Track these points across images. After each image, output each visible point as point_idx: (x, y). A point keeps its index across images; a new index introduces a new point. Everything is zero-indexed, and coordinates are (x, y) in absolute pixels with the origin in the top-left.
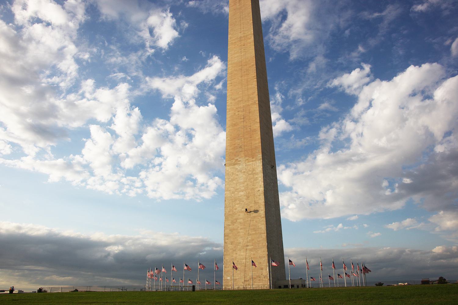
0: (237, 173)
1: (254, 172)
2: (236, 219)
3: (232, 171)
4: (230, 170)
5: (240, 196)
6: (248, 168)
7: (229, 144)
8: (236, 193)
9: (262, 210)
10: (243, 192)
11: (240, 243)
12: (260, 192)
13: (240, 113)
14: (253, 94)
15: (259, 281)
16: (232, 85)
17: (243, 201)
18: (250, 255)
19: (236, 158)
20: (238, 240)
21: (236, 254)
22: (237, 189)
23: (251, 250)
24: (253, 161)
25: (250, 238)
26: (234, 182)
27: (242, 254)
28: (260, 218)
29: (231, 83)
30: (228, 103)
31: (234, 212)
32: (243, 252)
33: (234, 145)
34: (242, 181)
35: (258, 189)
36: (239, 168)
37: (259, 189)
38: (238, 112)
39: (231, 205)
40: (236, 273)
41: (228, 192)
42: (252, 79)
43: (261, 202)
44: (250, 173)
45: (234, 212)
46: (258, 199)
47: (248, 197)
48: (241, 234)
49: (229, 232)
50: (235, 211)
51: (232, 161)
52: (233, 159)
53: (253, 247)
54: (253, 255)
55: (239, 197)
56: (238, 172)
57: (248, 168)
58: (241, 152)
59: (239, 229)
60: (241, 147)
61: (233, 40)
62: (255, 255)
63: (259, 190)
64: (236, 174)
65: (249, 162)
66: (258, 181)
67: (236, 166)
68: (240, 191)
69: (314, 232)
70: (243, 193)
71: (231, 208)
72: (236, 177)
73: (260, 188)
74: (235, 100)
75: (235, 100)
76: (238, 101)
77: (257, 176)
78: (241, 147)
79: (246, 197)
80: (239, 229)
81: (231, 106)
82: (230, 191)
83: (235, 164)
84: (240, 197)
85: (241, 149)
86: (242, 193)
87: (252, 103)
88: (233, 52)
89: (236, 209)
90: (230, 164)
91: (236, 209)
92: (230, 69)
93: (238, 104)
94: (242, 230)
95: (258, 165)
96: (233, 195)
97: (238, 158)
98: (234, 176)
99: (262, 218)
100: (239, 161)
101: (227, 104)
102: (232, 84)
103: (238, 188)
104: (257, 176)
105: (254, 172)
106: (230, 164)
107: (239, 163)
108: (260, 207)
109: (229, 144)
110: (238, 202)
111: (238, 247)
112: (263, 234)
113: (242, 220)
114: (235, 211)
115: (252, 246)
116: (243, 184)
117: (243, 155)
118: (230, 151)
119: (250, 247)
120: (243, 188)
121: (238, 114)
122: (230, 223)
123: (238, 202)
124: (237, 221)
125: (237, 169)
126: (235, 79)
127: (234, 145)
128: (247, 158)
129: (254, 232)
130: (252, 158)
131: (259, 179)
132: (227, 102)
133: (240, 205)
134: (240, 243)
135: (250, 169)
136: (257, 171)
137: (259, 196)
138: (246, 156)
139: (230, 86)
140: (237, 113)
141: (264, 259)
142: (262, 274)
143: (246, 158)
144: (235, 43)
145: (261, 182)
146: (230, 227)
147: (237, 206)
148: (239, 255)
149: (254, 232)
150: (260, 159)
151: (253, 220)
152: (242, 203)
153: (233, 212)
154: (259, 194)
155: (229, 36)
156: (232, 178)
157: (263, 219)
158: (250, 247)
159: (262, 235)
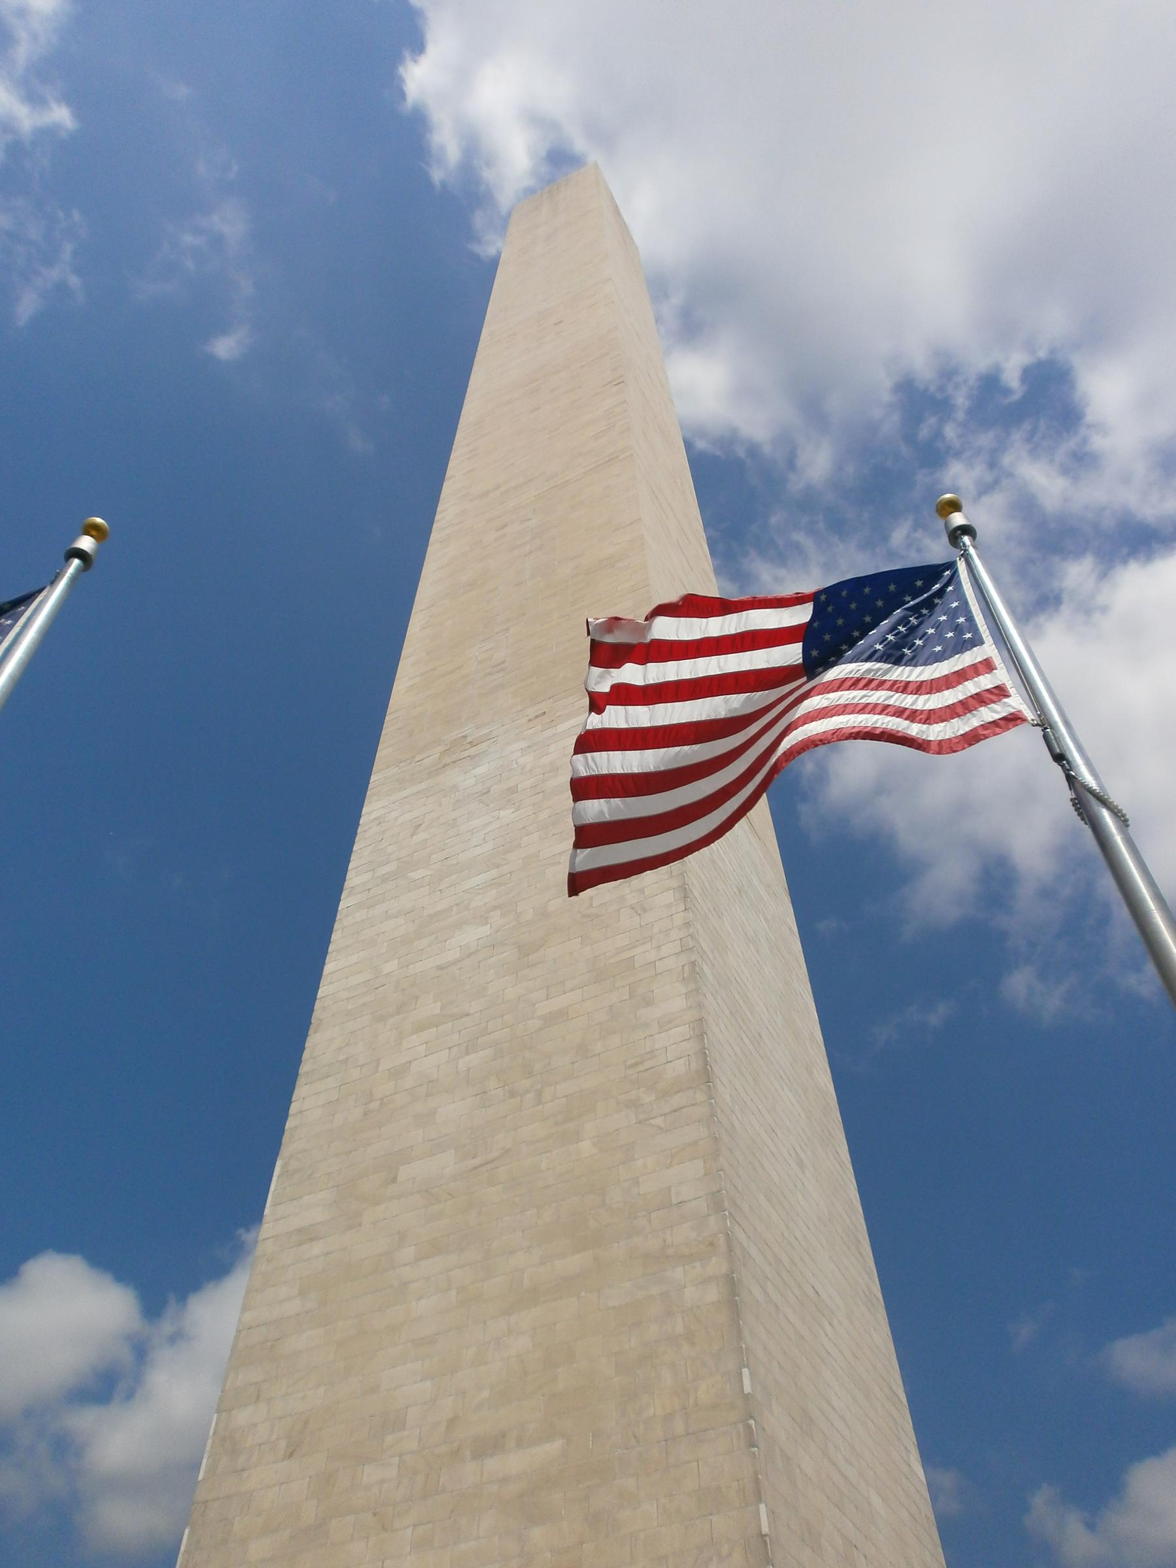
10: (485, 920)
26: (416, 875)
28: (648, 1098)
43: (652, 956)
51: (418, 758)
55: (440, 968)
70: (484, 931)
84: (455, 963)
91: (398, 1073)
96: (391, 966)
107: (472, 751)
108: (648, 1002)
116: (498, 866)
124: (394, 1180)
157: (678, 1100)
158: (515, 1462)
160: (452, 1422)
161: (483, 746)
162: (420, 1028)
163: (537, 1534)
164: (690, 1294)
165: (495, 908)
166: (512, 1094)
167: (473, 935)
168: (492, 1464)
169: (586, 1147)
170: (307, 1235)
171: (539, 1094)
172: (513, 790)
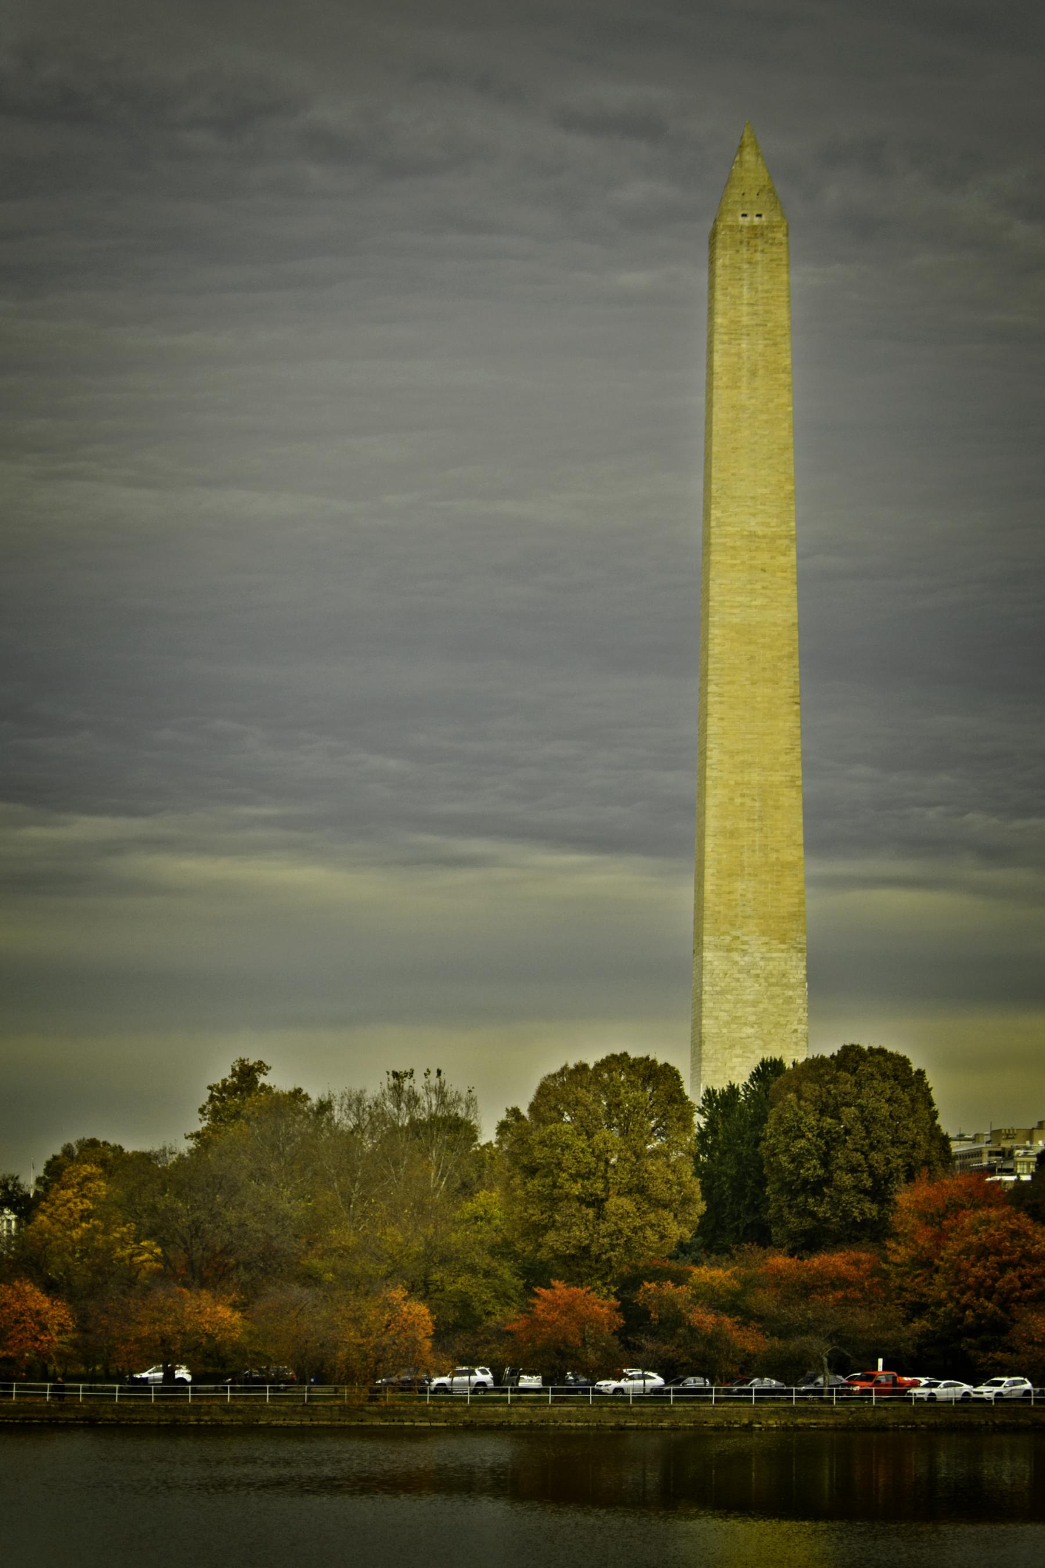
1: (785, 981)
3: (723, 967)
4: (716, 963)
5: (743, 1035)
13: (748, 801)
14: (786, 753)
24: (782, 951)
26: (729, 997)
29: (720, 695)
36: (743, 963)
37: (796, 1027)
38: (743, 796)
39: (719, 1056)
41: (712, 1022)
44: (773, 980)
52: (727, 933)
56: (739, 972)
57: (769, 968)
58: (749, 917)
61: (726, 536)
63: (796, 1031)
65: (769, 951)
66: (793, 1006)
67: (736, 956)
68: (745, 1024)
69: (988, 1179)
70: (753, 1030)
72: (734, 984)
74: (732, 754)
75: (732, 754)
76: (742, 762)
77: (790, 993)
81: (721, 771)
82: (717, 1018)
83: (729, 950)
86: (749, 1031)
87: (783, 778)
88: (724, 581)
89: (733, 1068)
90: (716, 946)
91: (733, 1068)
92: (717, 641)
95: (794, 963)
96: (725, 1031)
98: (727, 980)
100: (744, 943)
101: (709, 762)
102: (724, 699)
104: (790, 993)
105: (785, 981)
106: (716, 946)
117: (754, 929)
118: (717, 909)
121: (742, 804)
123: (738, 1051)
126: (732, 683)
127: (729, 893)
130: (781, 943)
132: (709, 753)
135: (774, 972)
136: (793, 981)
138: (763, 933)
139: (716, 702)
140: (738, 801)
143: (765, 939)
144: (734, 548)
147: (735, 1060)
152: (749, 1055)
156: (723, 984)
162: (737, 1057)
172: (758, 976)
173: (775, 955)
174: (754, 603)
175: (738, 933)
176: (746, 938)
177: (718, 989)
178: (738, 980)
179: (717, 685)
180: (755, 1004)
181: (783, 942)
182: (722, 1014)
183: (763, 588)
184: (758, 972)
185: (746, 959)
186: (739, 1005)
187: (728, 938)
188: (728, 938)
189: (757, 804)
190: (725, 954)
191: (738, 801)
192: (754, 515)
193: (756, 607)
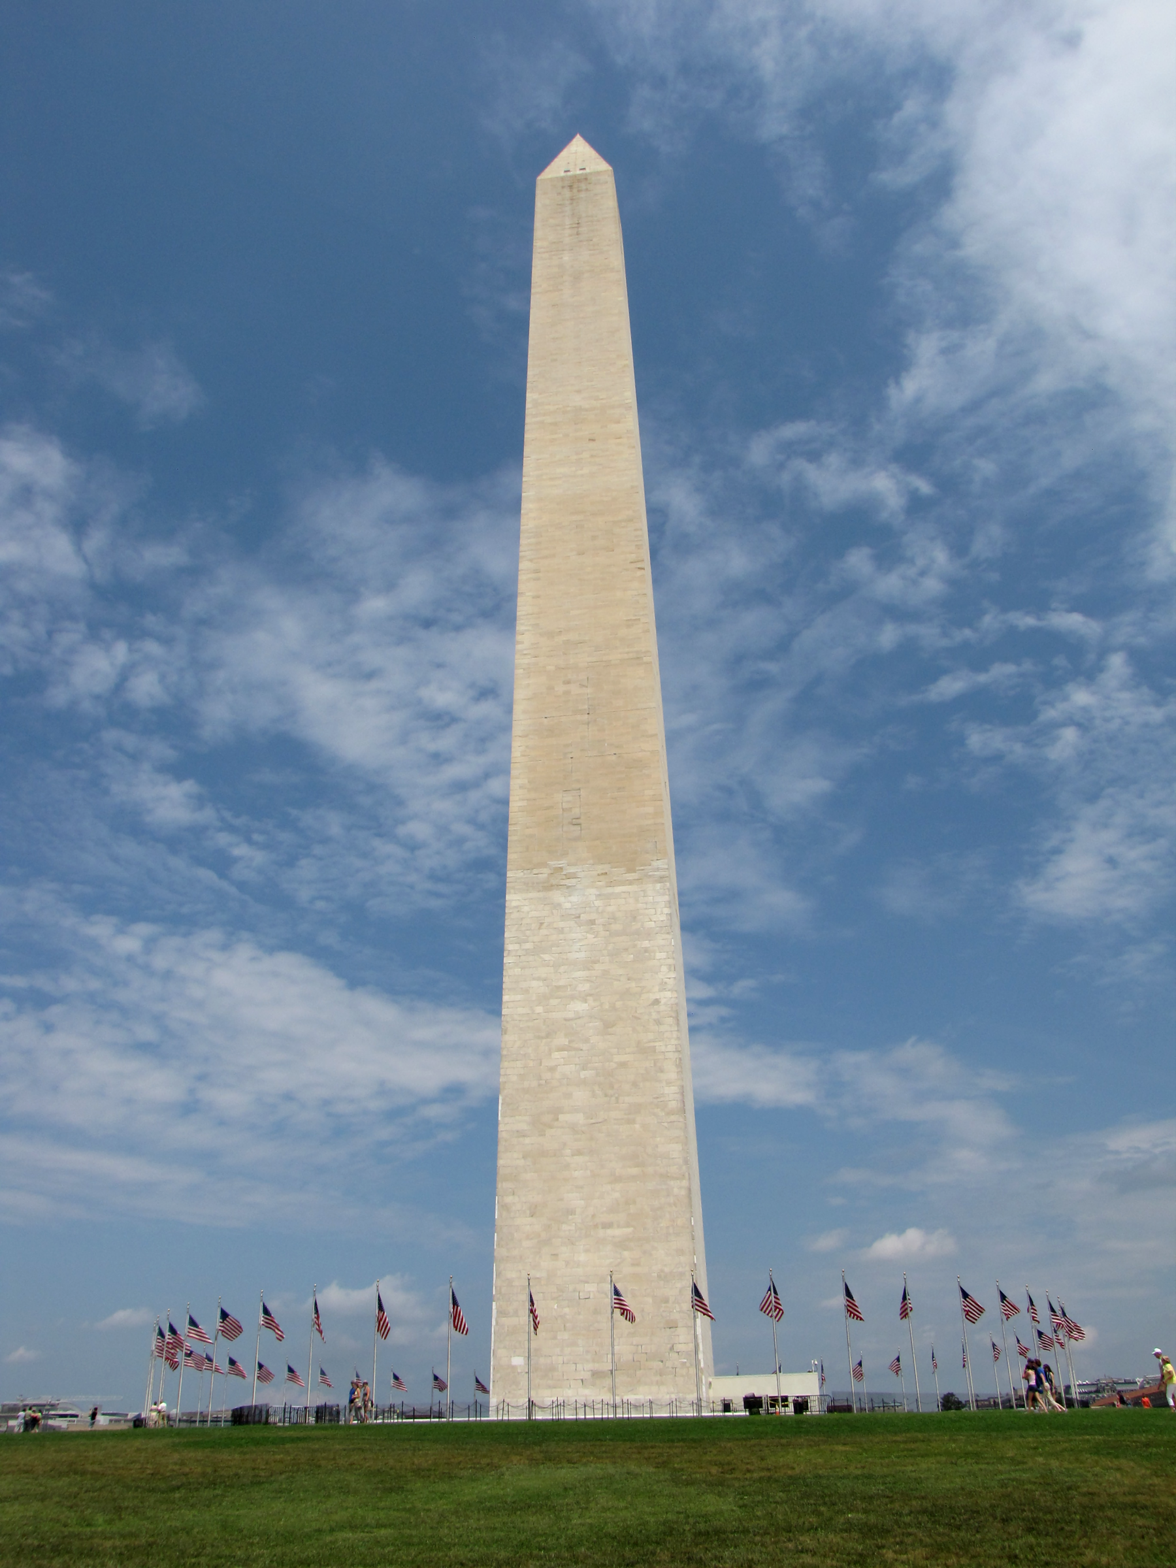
0: (561, 924)
2: (556, 1111)
4: (526, 909)
5: (571, 1015)
6: (610, 909)
7: (525, 803)
8: (553, 1002)
9: (669, 1083)
11: (573, 1212)
12: (662, 1008)
15: (658, 1378)
16: (538, 579)
17: (587, 1040)
18: (619, 1264)
19: (554, 863)
20: (562, 1200)
21: (555, 1256)
22: (558, 988)
23: (622, 1244)
24: (631, 883)
25: (617, 1195)
26: (546, 957)
27: (582, 1257)
28: (662, 1114)
29: (537, 571)
30: (522, 643)
31: (543, 1082)
32: (587, 1251)
33: (548, 808)
34: (582, 955)
35: (653, 997)
36: (568, 905)
38: (568, 682)
40: (555, 1338)
41: (519, 997)
42: (626, 570)
43: (663, 1049)
44: (616, 927)
45: (543, 1082)
46: (651, 1036)
47: (607, 1027)
48: (576, 1174)
49: (521, 1162)
50: (548, 1075)
51: (535, 871)
52: (544, 865)
53: (630, 1230)
54: (633, 1265)
55: (566, 1020)
56: (563, 917)
57: (610, 909)
59: (568, 1152)
60: (576, 822)
62: (638, 1265)
63: (657, 1002)
64: (555, 925)
65: (610, 884)
67: (557, 896)
68: (573, 998)
70: (585, 1006)
71: (531, 1064)
73: (660, 991)
77: (646, 944)
78: (576, 822)
79: (598, 1024)
80: (568, 1152)
82: (527, 991)
83: (548, 887)
85: (578, 828)
86: (580, 1007)
87: (626, 656)
91: (552, 1069)
93: (565, 654)
94: (579, 1159)
96: (539, 1009)
97: (562, 863)
98: (544, 932)
99: (669, 1114)
101: (519, 647)
103: (561, 983)
104: (646, 944)
108: (662, 1071)
109: (525, 803)
110: (561, 1040)
111: (564, 1227)
112: (677, 1179)
113: (579, 1118)
114: (548, 1075)
115: (628, 1225)
119: (617, 1232)
120: (585, 987)
121: (567, 693)
122: (524, 1126)
123: (561, 1040)
125: (559, 905)
127: (548, 808)
128: (601, 867)
129: (635, 1171)
131: (659, 955)
133: (573, 1053)
134: (573, 1212)
137: (658, 1022)
140: (560, 688)
141: (679, 1285)
142: (672, 1348)
143: (600, 868)
144: (555, 424)
145: (664, 969)
146: (527, 1141)
147: (556, 1055)
148: (567, 1263)
149: (635, 1171)
150: (661, 879)
151: (633, 1122)
153: (540, 1078)
154: (654, 1016)
155: (530, 396)
157: (673, 1118)
158: (617, 1232)
159: (672, 1183)
160: (593, 1216)
161: (572, 882)
163: (626, 1254)
164: (676, 1190)
165: (591, 995)
166: (606, 1095)
167: (580, 1007)
168: (609, 1232)
169: (637, 1126)
170: (522, 1134)
171: (617, 1098)
172: (592, 922)
173: (618, 889)
174: (580, 472)
175: (562, 863)
176: (572, 870)
177: (528, 946)
178: (561, 931)
179: (531, 560)
180: (589, 964)
181: (631, 870)
182: (535, 984)
183: (592, 456)
184: (593, 916)
185: (574, 899)
186: (562, 969)
187: (546, 871)
188: (546, 871)
189: (589, 690)
190: (541, 895)
191: (560, 688)
192: (579, 392)
193: (582, 476)
